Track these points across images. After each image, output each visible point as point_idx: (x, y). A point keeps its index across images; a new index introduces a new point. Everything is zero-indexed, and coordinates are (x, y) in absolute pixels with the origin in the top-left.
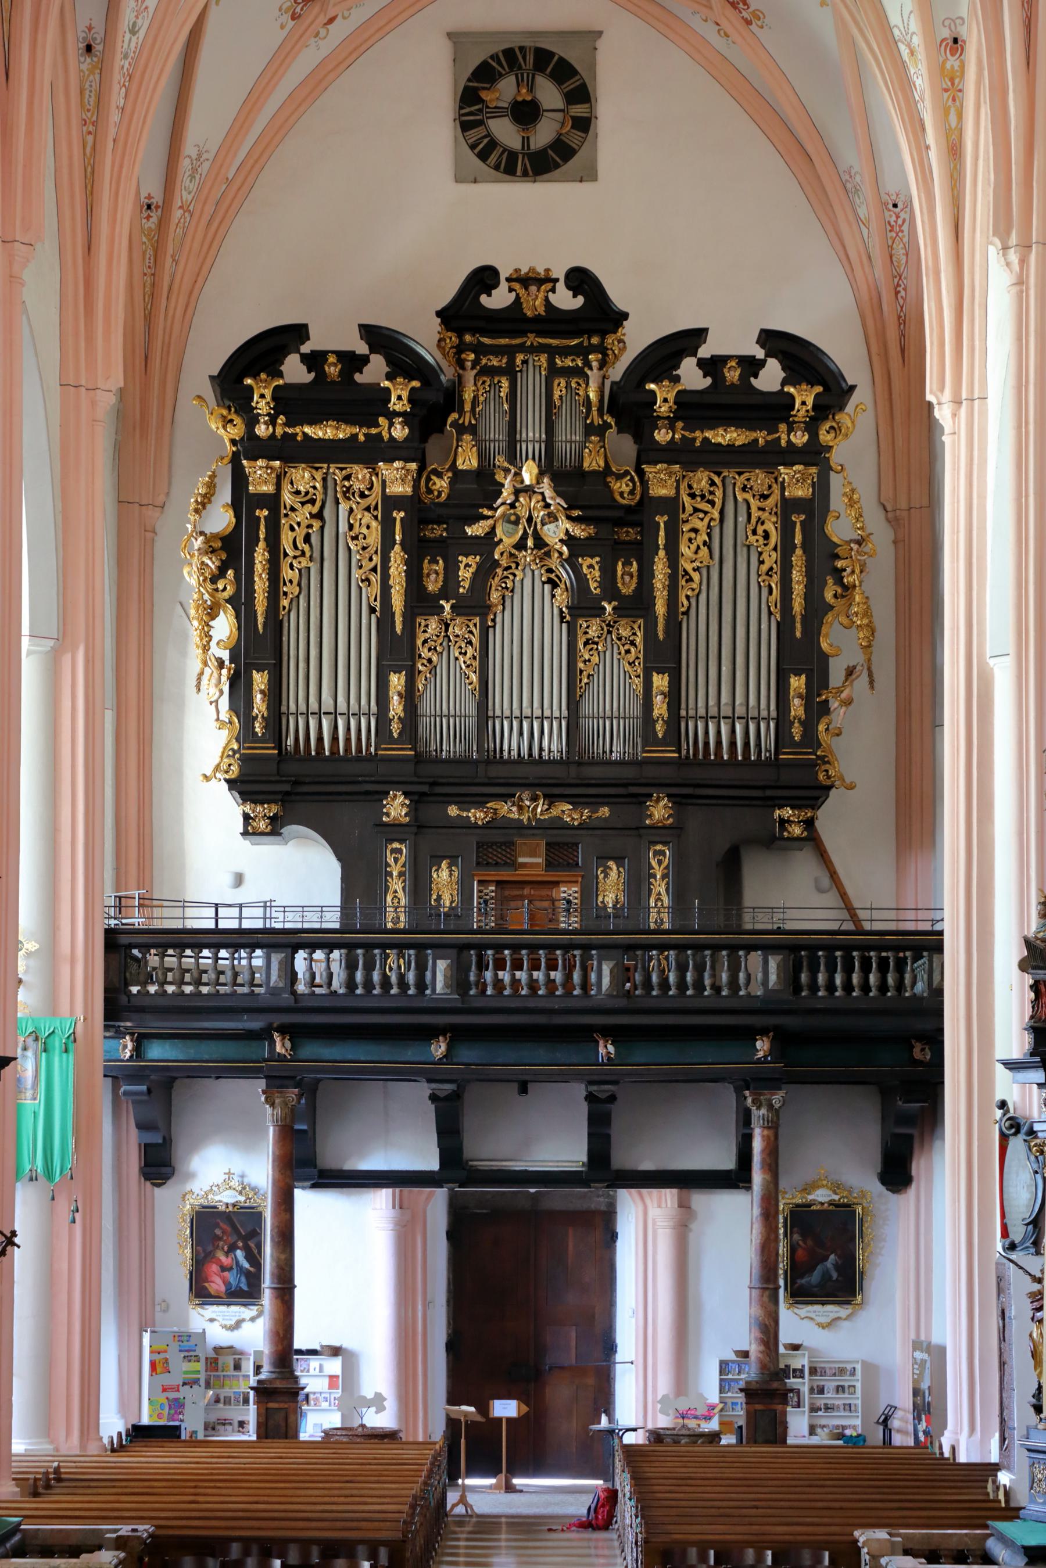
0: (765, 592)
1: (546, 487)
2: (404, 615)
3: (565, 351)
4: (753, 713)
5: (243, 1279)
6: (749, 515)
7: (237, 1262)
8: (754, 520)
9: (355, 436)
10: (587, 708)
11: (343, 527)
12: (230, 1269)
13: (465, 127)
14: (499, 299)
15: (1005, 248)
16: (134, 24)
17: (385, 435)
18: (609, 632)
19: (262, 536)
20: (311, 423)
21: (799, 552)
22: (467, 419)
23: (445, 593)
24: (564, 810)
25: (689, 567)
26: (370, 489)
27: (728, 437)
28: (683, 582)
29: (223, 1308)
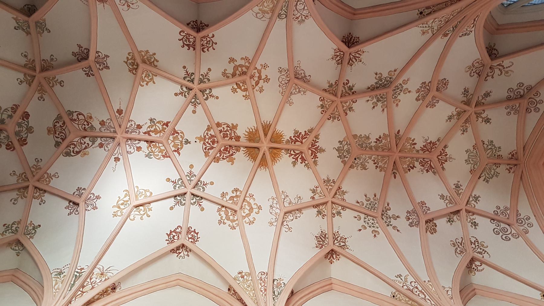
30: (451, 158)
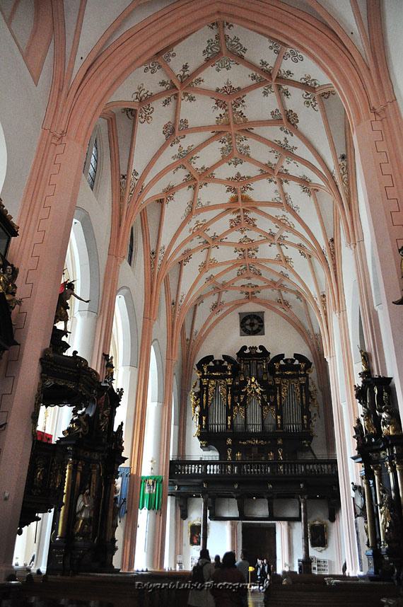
1: (256, 383)
3: (259, 360)
10: (265, 422)
30: (228, 83)
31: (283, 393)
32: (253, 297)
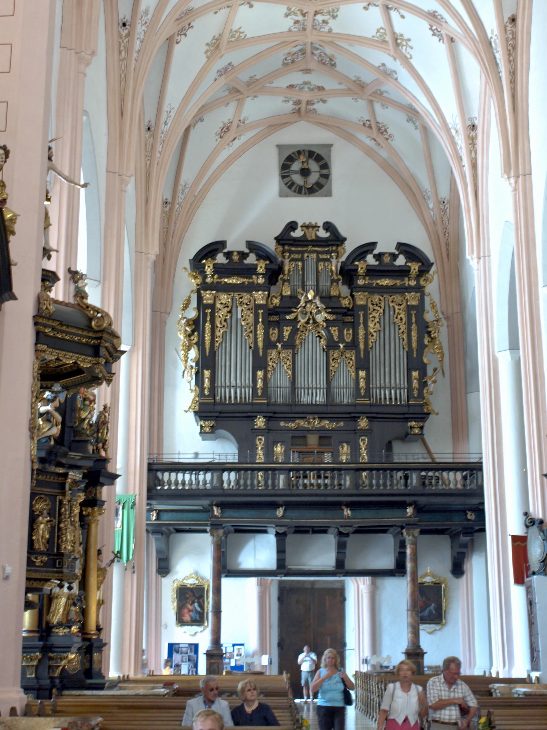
0: (401, 340)
1: (317, 301)
2: (263, 349)
3: (323, 253)
4: (398, 386)
5: (198, 615)
6: (394, 312)
7: (195, 608)
8: (396, 313)
9: (244, 283)
10: (334, 384)
11: (239, 316)
12: (192, 611)
13: (283, 177)
14: (298, 233)
15: (509, 178)
16: (166, 121)
17: (255, 281)
18: (342, 355)
19: (208, 319)
20: (227, 277)
21: (414, 325)
22: (286, 277)
23: (279, 341)
24: (325, 423)
25: (372, 331)
26: (250, 302)
27: (386, 282)
28: (370, 336)
29: (189, 627)
31: (371, 325)
32: (308, 112)
